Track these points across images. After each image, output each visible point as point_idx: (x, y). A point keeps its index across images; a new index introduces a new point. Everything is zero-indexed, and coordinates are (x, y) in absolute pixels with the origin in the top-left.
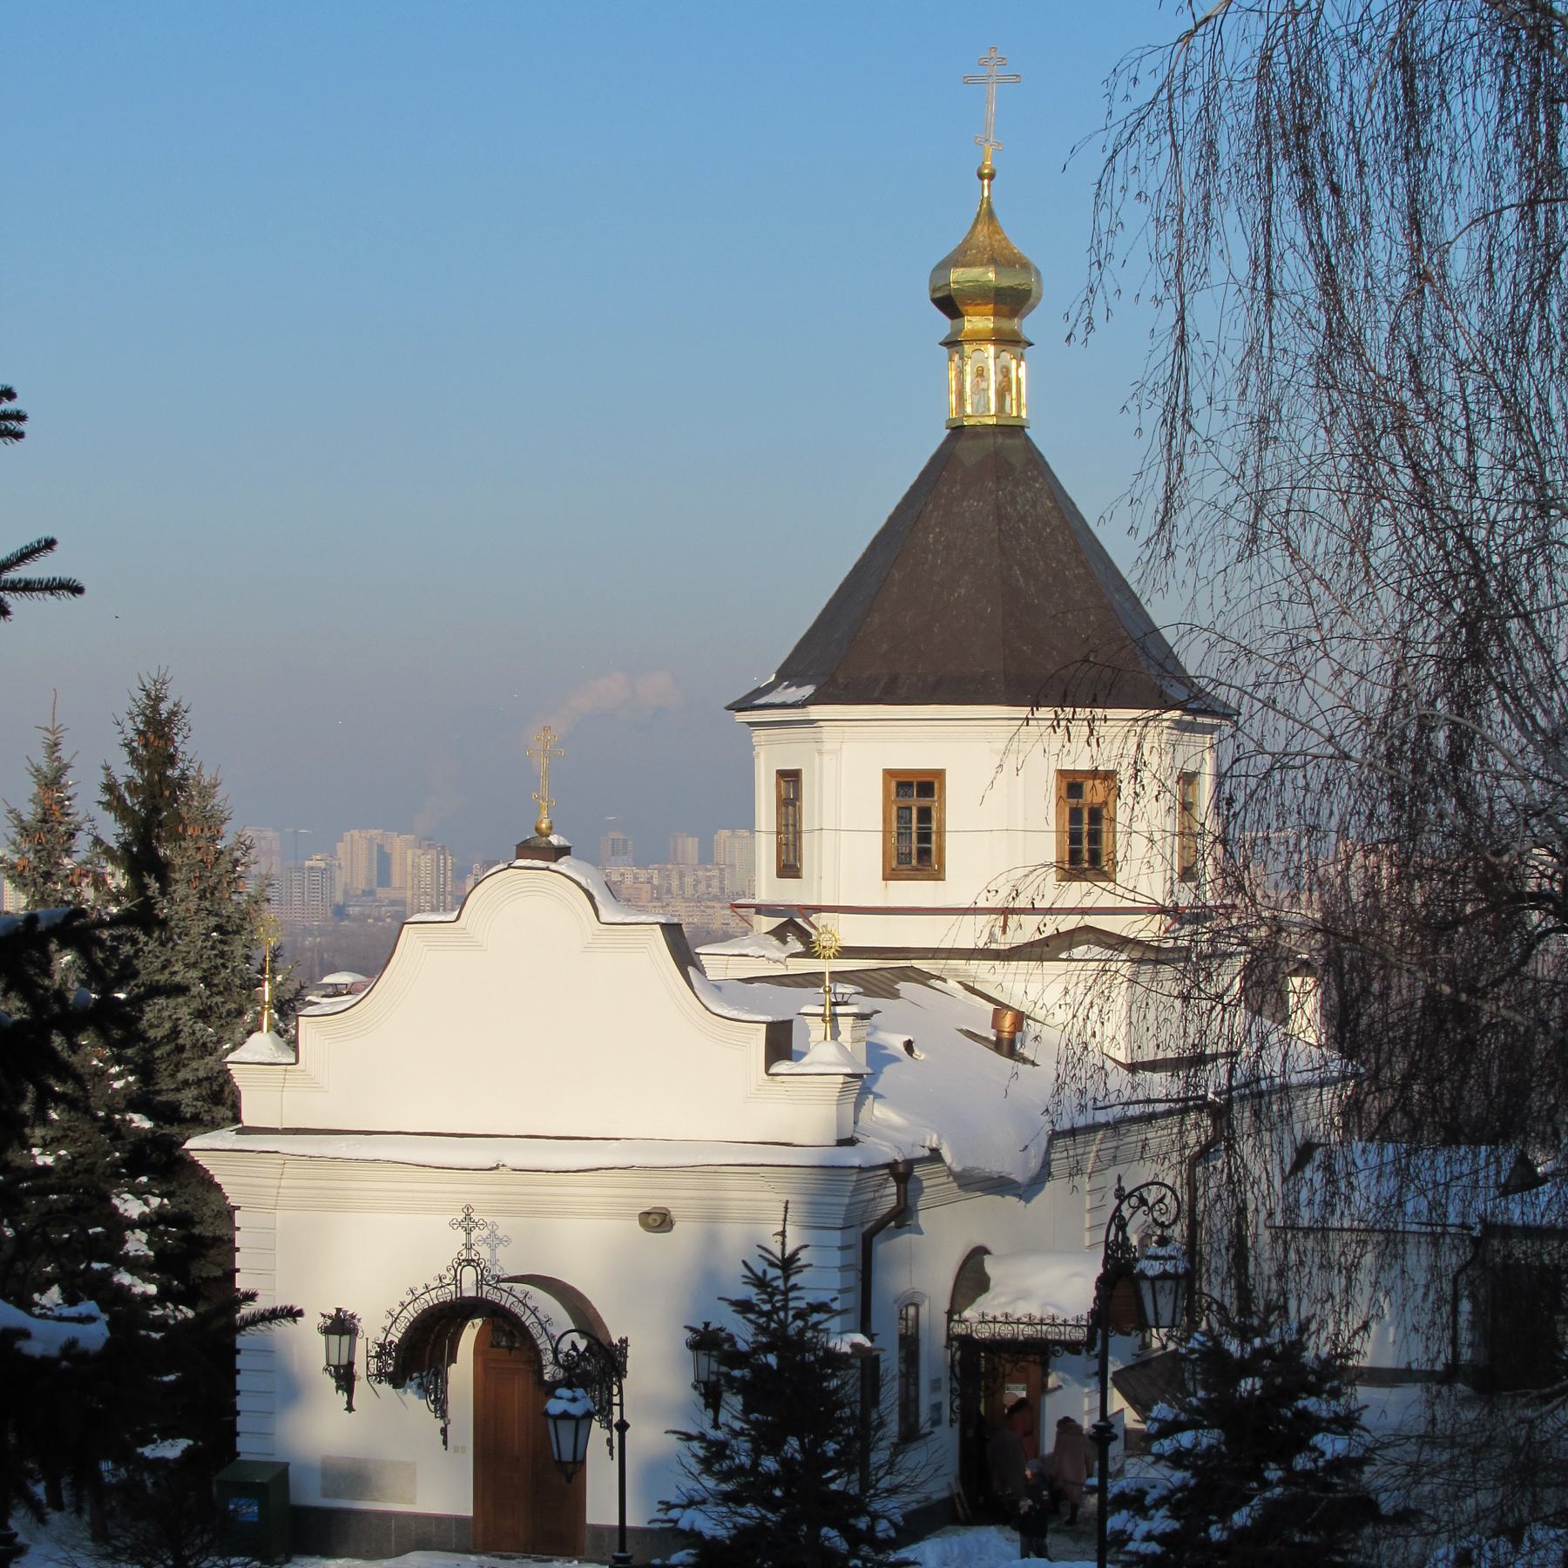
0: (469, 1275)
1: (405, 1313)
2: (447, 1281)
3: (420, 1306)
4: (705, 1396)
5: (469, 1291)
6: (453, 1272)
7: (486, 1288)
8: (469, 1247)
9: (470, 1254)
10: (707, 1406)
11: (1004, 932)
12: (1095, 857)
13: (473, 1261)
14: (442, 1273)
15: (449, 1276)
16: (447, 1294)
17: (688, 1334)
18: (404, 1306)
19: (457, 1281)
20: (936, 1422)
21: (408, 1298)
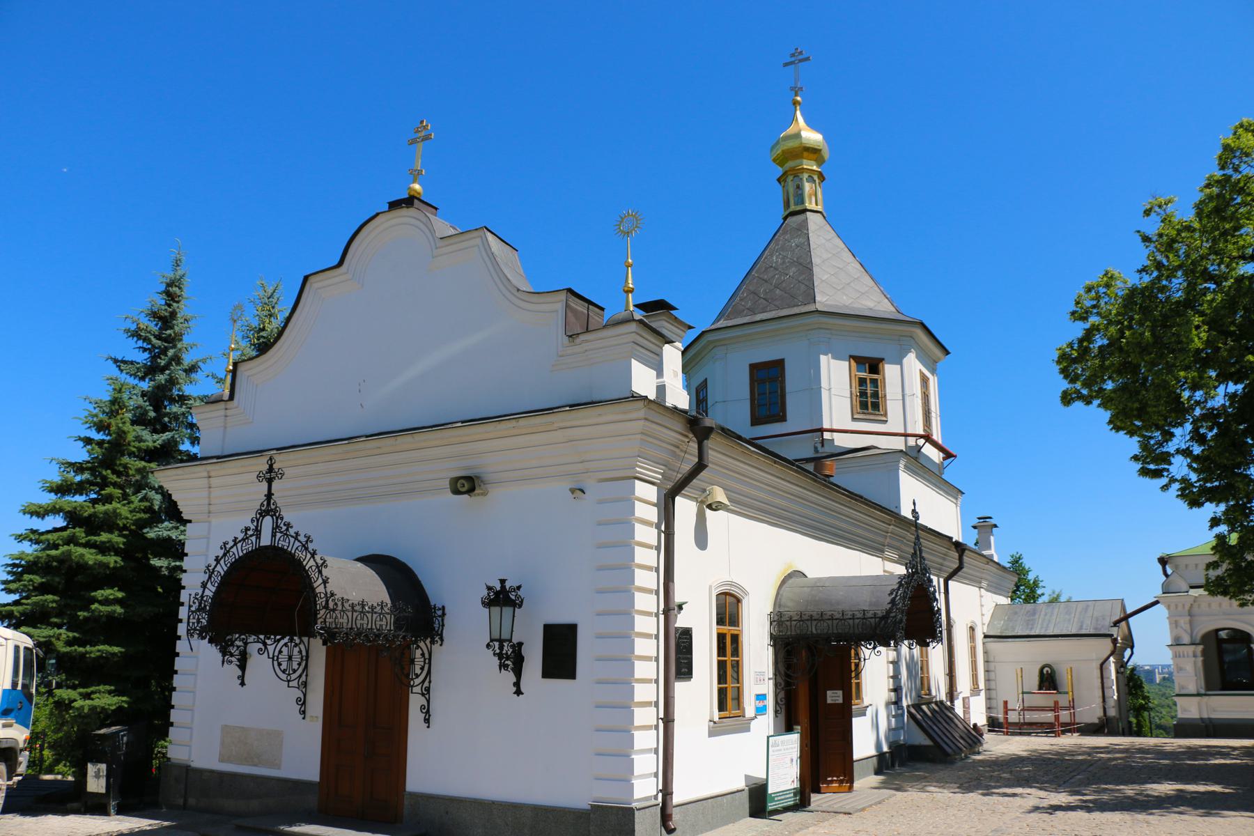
0: (268, 522)
1: (218, 568)
2: (250, 533)
3: (230, 559)
5: (266, 540)
6: (255, 524)
7: (279, 535)
8: (269, 495)
9: (269, 504)
10: (503, 666)
11: (823, 446)
12: (876, 406)
13: (272, 510)
14: (249, 524)
15: (253, 527)
16: (249, 547)
17: (485, 592)
18: (217, 560)
19: (258, 532)
20: (760, 711)
21: (221, 553)
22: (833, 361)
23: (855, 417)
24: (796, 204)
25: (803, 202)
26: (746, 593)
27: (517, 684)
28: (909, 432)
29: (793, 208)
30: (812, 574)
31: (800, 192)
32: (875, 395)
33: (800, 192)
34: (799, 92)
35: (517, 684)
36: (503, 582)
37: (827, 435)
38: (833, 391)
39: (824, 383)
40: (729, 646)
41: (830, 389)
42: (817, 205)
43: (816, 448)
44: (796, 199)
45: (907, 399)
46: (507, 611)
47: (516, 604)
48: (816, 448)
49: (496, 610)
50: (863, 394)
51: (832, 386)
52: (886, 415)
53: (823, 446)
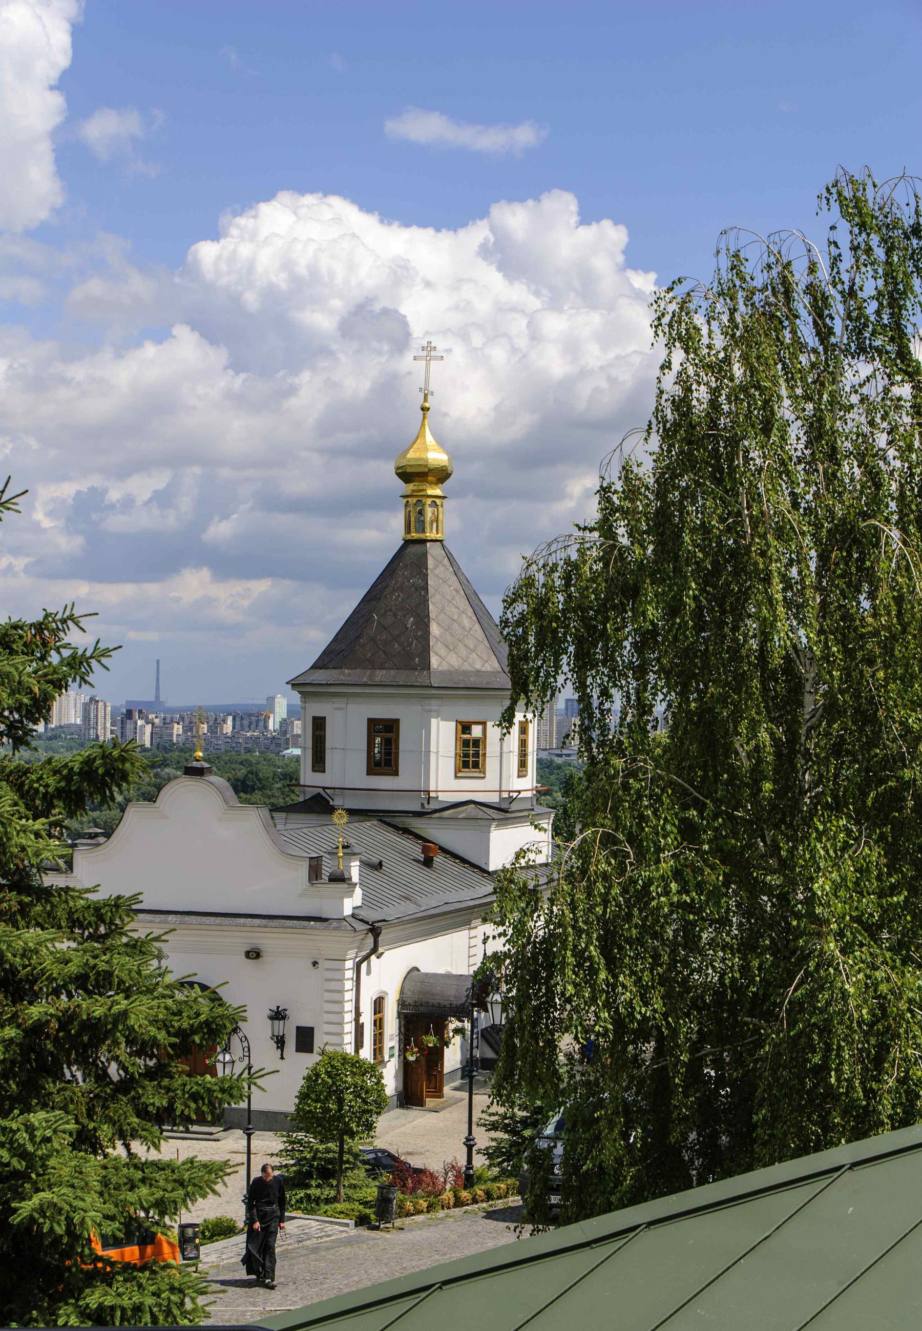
4: (277, 1043)
10: (278, 1048)
11: (428, 803)
12: (476, 765)
17: (269, 1012)
20: (392, 1056)
22: (442, 723)
23: (459, 775)
24: (417, 532)
25: (424, 531)
26: (387, 994)
27: (282, 1054)
28: (503, 789)
29: (415, 535)
30: (424, 970)
31: (422, 518)
32: (476, 755)
33: (422, 518)
34: (429, 397)
35: (282, 1054)
36: (278, 1007)
37: (432, 794)
38: (440, 754)
39: (433, 748)
40: (379, 1024)
41: (438, 752)
42: (437, 533)
43: (422, 805)
44: (418, 525)
45: (504, 755)
46: (282, 1022)
47: (284, 1018)
48: (422, 805)
49: (276, 1022)
50: (466, 755)
51: (440, 750)
52: (484, 773)
53: (428, 803)
